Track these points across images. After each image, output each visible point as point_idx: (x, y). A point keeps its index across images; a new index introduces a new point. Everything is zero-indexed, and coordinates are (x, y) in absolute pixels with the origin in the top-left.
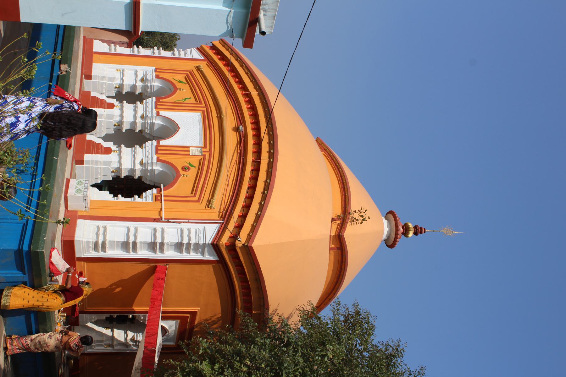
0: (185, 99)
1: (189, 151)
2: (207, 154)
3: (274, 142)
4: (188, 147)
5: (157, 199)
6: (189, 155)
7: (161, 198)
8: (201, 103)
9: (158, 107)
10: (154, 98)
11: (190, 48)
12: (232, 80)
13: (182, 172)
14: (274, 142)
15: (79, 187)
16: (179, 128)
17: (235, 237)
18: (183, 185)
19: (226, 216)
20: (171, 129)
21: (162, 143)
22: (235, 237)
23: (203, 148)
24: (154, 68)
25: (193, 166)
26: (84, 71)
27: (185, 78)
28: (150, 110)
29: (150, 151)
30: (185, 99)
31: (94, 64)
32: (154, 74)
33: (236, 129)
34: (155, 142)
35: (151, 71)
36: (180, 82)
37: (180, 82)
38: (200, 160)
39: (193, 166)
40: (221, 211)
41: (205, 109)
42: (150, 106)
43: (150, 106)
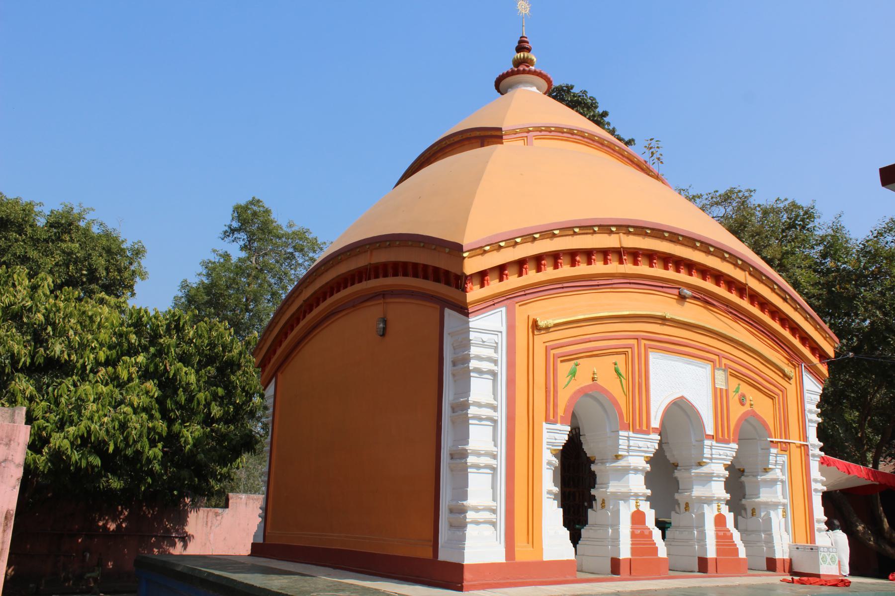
0: (617, 371)
1: (721, 389)
2: (724, 361)
3: (727, 253)
4: (715, 389)
5: (785, 447)
6: (727, 391)
7: (785, 443)
8: (631, 347)
9: (644, 428)
10: (621, 433)
11: (467, 330)
12: (582, 269)
13: (747, 408)
14: (727, 253)
15: (829, 560)
16: (682, 397)
17: (823, 356)
18: (764, 407)
19: (795, 357)
20: (680, 410)
21: (710, 431)
22: (823, 356)
23: (714, 367)
24: (545, 426)
25: (738, 388)
26: (570, 578)
27: (562, 361)
28: (649, 444)
29: (721, 452)
30: (617, 371)
31: (545, 559)
32: (558, 426)
33: (682, 298)
34: (707, 442)
35: (550, 431)
36: (573, 374)
37: (573, 374)
38: (732, 375)
39: (738, 388)
40: (787, 362)
41: (643, 342)
42: (641, 444)
43: (641, 444)
